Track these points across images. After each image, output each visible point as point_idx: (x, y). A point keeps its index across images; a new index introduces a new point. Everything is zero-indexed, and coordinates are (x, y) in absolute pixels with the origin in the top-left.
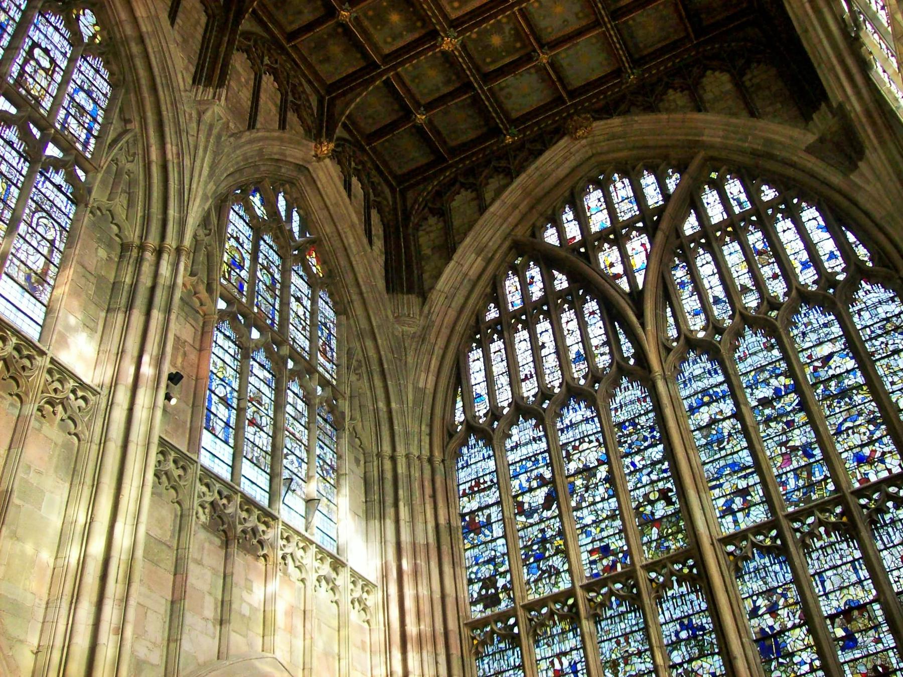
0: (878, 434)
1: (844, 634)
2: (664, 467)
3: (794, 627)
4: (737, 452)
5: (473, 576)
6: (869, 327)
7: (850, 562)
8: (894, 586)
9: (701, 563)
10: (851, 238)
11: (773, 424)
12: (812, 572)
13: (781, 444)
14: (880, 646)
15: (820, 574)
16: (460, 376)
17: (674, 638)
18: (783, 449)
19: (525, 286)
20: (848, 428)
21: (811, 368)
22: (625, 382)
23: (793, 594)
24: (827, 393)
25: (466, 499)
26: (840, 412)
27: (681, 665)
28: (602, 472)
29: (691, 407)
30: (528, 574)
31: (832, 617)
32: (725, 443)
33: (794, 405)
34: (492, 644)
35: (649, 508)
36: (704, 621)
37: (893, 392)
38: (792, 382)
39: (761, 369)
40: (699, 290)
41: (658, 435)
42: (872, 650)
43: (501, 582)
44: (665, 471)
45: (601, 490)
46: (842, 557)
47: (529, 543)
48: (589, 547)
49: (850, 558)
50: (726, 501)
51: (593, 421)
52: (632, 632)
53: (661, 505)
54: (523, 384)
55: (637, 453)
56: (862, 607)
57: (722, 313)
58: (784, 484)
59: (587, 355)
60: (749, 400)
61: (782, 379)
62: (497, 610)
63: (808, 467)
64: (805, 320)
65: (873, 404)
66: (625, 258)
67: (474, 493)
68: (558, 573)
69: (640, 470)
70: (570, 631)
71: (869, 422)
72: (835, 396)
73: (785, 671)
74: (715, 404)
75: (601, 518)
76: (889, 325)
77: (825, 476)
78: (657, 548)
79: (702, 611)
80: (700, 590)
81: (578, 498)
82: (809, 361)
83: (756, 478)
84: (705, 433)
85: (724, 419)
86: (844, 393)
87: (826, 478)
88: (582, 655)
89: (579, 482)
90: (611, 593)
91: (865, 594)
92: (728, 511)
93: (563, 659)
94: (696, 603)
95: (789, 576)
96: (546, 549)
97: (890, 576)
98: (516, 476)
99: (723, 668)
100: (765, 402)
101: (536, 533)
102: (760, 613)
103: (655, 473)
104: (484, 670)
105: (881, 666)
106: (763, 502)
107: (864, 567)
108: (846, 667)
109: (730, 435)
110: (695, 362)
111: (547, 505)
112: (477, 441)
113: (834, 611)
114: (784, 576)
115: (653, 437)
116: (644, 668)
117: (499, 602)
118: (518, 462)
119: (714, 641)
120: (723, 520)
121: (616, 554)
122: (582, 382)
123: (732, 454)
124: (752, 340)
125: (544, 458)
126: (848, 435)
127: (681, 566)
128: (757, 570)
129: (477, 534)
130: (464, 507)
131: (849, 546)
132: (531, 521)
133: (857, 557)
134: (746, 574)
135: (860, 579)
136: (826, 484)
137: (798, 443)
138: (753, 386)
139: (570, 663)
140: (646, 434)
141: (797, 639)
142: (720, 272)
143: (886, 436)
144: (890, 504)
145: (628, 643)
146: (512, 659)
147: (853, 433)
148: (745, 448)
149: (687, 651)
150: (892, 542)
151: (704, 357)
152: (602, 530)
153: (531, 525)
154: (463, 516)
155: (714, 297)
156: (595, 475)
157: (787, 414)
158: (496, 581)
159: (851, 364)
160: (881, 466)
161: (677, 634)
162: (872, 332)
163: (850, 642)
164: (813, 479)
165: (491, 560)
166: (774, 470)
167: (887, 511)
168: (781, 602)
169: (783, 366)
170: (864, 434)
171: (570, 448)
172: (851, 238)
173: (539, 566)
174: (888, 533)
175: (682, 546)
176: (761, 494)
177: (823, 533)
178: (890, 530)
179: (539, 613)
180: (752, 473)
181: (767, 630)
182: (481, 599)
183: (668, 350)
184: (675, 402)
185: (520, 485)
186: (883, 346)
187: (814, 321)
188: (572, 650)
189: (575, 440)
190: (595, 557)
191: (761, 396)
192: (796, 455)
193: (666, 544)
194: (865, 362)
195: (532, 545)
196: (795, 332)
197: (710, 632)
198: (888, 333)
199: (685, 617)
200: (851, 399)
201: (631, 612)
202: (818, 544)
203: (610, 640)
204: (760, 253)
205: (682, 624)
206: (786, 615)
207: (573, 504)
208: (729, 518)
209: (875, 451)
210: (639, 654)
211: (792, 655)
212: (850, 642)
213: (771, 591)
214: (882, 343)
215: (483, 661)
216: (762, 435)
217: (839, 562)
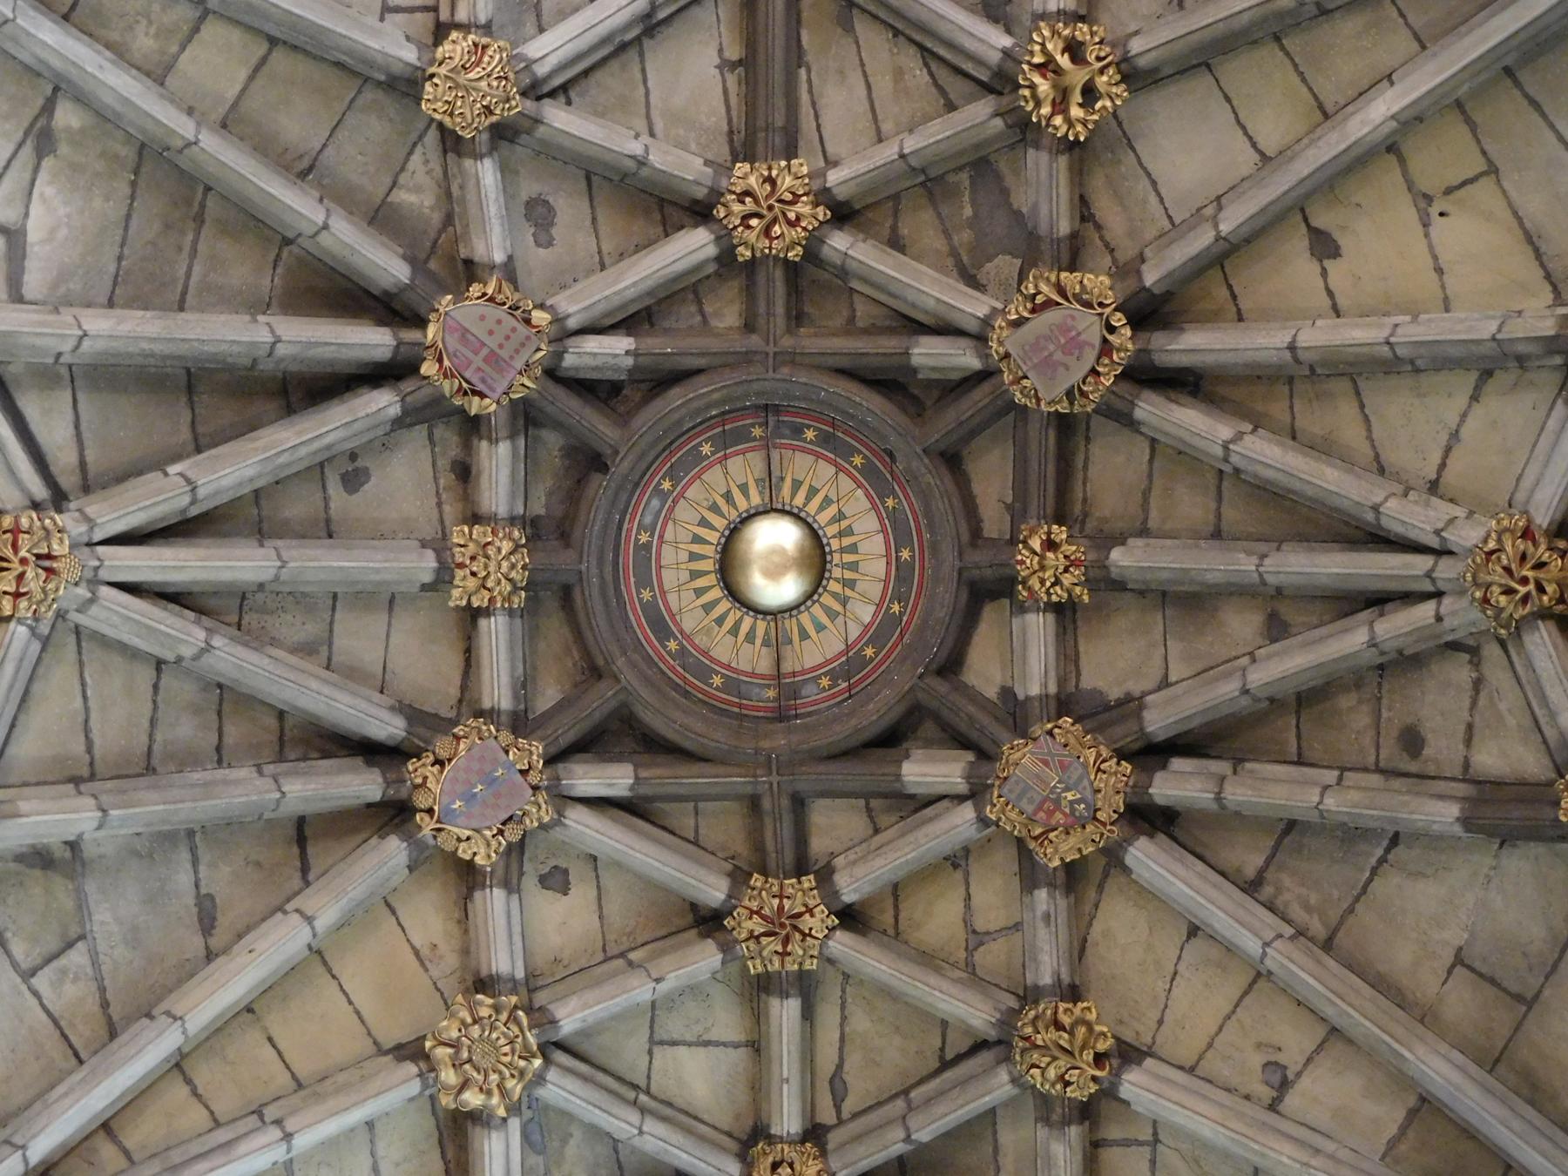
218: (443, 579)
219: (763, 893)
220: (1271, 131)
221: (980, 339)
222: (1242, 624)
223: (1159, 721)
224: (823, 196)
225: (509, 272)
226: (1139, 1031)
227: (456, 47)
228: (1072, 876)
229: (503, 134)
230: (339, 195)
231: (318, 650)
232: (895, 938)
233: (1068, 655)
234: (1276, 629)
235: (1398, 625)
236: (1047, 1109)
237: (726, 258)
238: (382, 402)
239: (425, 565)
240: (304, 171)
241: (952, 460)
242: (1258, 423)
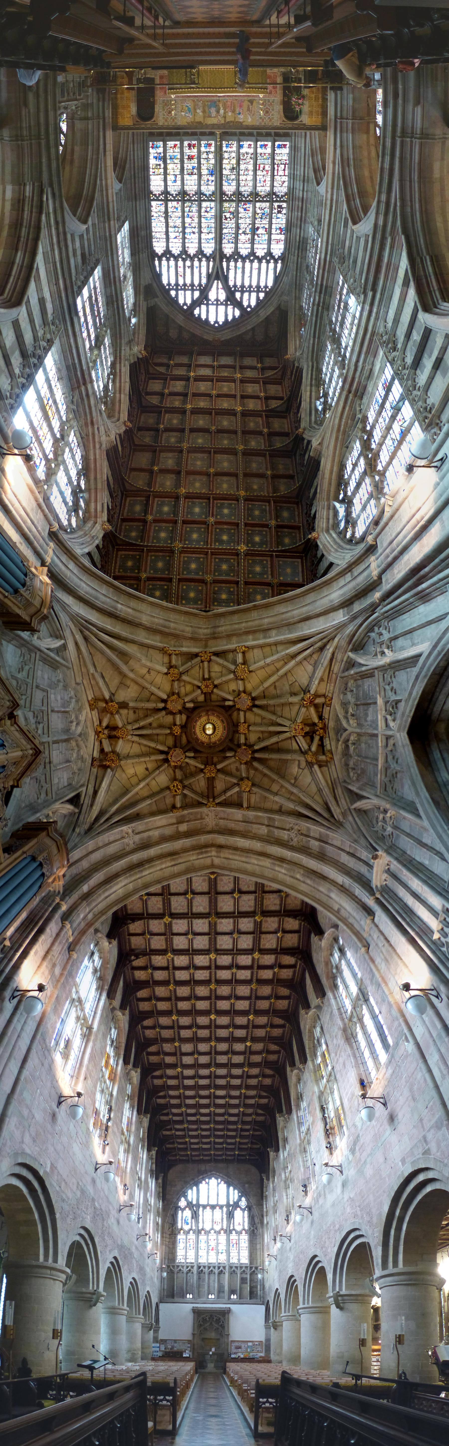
9: (221, 197)
16: (276, 279)
19: (249, 299)
23: (202, 182)
28: (240, 231)
40: (200, 274)
43: (276, 211)
57: (196, 263)
59: (236, 267)
66: (217, 293)
83: (203, 214)
86: (175, 227)
89: (248, 231)
91: (186, 177)
92: (211, 208)
100: (194, 233)
111: (258, 228)
124: (192, 251)
141: (204, 172)
159: (170, 234)
169: (186, 241)
183: (213, 258)
184: (216, 243)
194: (167, 233)
212: (193, 168)
213: (208, 185)
218: (249, 726)
219: (210, 690)
220: (153, 783)
221: (186, 757)
222: (154, 725)
223: (164, 713)
224: (204, 773)
225: (241, 764)
226: (165, 676)
227: (248, 789)
228: (173, 694)
229: (242, 779)
230: (261, 772)
231: (263, 718)
232: (194, 685)
233: (174, 719)
234: (150, 724)
235: (137, 726)
236: (176, 667)
237: (215, 765)
238: (256, 747)
239: (251, 728)
240: (265, 775)
241: (189, 742)
242: (153, 748)
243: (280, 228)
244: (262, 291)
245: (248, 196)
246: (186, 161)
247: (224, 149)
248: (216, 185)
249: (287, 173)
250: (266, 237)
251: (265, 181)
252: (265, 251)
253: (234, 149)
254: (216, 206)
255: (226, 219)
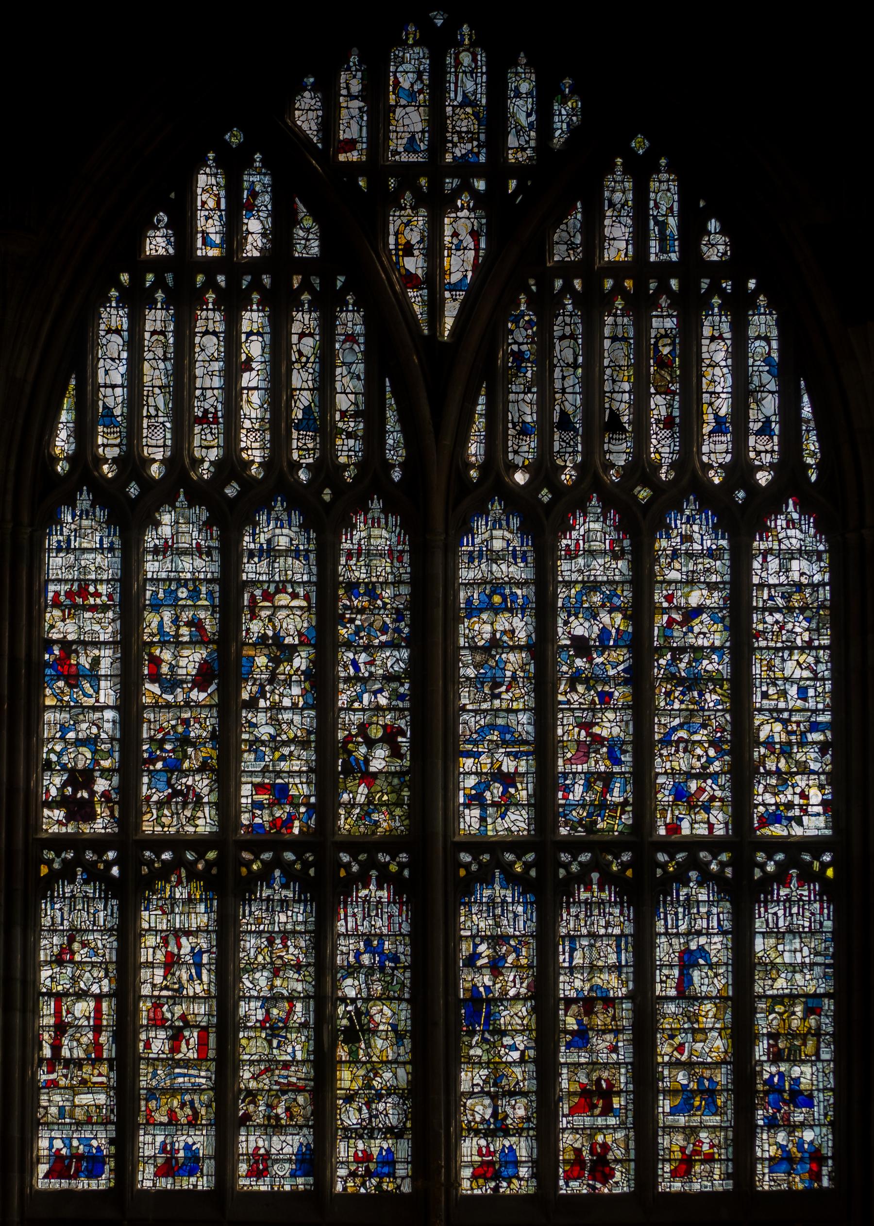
0: (716, 766)
1: (576, 1027)
2: (402, 690)
3: (517, 997)
4: (516, 711)
5: (53, 757)
6: (770, 586)
7: (616, 936)
8: (658, 987)
10: (807, 411)
11: (581, 688)
12: (563, 931)
13: (581, 726)
14: (614, 1056)
15: (572, 939)
17: (352, 959)
18: (583, 733)
20: (681, 740)
21: (665, 617)
22: (376, 505)
24: (673, 669)
25: (57, 613)
26: (680, 710)
27: (353, 1001)
29: (469, 601)
30: (149, 788)
31: (569, 1001)
32: (504, 688)
33: (621, 668)
34: (72, 881)
35: (363, 750)
36: (401, 949)
37: (760, 710)
38: (630, 630)
39: (592, 586)
41: (406, 630)
42: (603, 1057)
43: (101, 785)
44: (401, 697)
45: (296, 691)
46: (608, 925)
47: (160, 736)
48: (258, 780)
49: (617, 931)
50: (478, 783)
51: (307, 558)
52: (294, 932)
53: (381, 752)
54: (197, 429)
55: (367, 648)
56: (609, 1002)
58: (568, 789)
60: (560, 630)
61: (618, 617)
62: (86, 829)
63: (607, 778)
64: (684, 529)
65: (728, 717)
67: (75, 606)
68: (198, 803)
69: (364, 681)
70: (201, 900)
71: (712, 743)
72: (681, 681)
73: (488, 1051)
74: (507, 615)
75: (284, 737)
76: (797, 597)
77: (626, 799)
78: (360, 818)
79: (401, 934)
80: (407, 903)
81: (255, 689)
82: (665, 605)
84: (478, 658)
85: (512, 649)
87: (625, 803)
88: (214, 943)
89: (261, 661)
90: (277, 862)
92: (477, 799)
93: (183, 940)
94: (396, 919)
95: (532, 926)
96: (186, 756)
97: (658, 972)
98: (156, 607)
99: (409, 1022)
100: (581, 646)
101: (173, 722)
102: (479, 963)
103: (386, 694)
104: (52, 918)
105: (607, 1081)
106: (529, 805)
107: (630, 949)
108: (565, 1071)
109: (514, 677)
110: (497, 524)
111: (201, 680)
112: (93, 506)
113: (573, 994)
114: (525, 922)
115: (397, 630)
116: (300, 989)
117: (91, 817)
118: (164, 580)
119: (407, 982)
120: (467, 811)
121: (297, 806)
122: (303, 476)
123: (509, 711)
125: (210, 593)
126: (677, 751)
127: (388, 859)
128: (492, 903)
129: (71, 686)
130: (52, 627)
131: (621, 913)
132: (170, 698)
133: (627, 931)
134: (475, 902)
135: (620, 962)
136: (623, 812)
137: (605, 733)
138: (573, 611)
139: (193, 949)
140: (388, 620)
142: (587, 366)
143: (725, 773)
144: (693, 875)
145: (286, 946)
146: (102, 914)
147: (685, 750)
148: (530, 710)
149: (367, 984)
150: (677, 927)
151: (515, 522)
152: (283, 758)
153: (168, 706)
154: (49, 643)
155: (563, 414)
156: (290, 660)
157: (606, 680)
158: (93, 782)
160: (703, 816)
161: (358, 954)
162: (771, 598)
163: (581, 1038)
164: (608, 797)
165: (91, 742)
166: (560, 762)
167: (686, 883)
168: (510, 959)
169: (625, 595)
170: (699, 757)
171: (258, 592)
172: (807, 411)
173: (169, 780)
174: (676, 914)
175: (396, 829)
176: (531, 791)
177: (595, 881)
178: (681, 910)
179: (158, 856)
180: (527, 754)
181: (482, 989)
182: (62, 802)
185: (161, 624)
186: (776, 628)
187: (696, 536)
188: (199, 929)
189: (269, 582)
190: (263, 798)
191: (579, 631)
192: (597, 752)
193: (375, 817)
195: (163, 741)
196: (664, 543)
197: (405, 968)
198: (790, 610)
199: (376, 935)
200: (701, 694)
201: (299, 901)
202: (584, 896)
203: (260, 933)
204: (663, 363)
205: (368, 943)
206: (511, 978)
207: (245, 696)
208: (476, 812)
209: (704, 790)
210: (298, 967)
211: (504, 1033)
212: (581, 1038)
214: (777, 622)
215: (53, 903)
216: (561, 698)
217: (602, 931)
243: (73, 679)
244: (159, 264)
245: (265, 876)
246: (622, 1079)
247: (403, 1149)
248: (452, 937)
249: (48, 1009)
250: (152, 620)
251: (171, 963)
252: (151, 540)
253: (343, 1150)
254: (452, 816)
255: (390, 736)
